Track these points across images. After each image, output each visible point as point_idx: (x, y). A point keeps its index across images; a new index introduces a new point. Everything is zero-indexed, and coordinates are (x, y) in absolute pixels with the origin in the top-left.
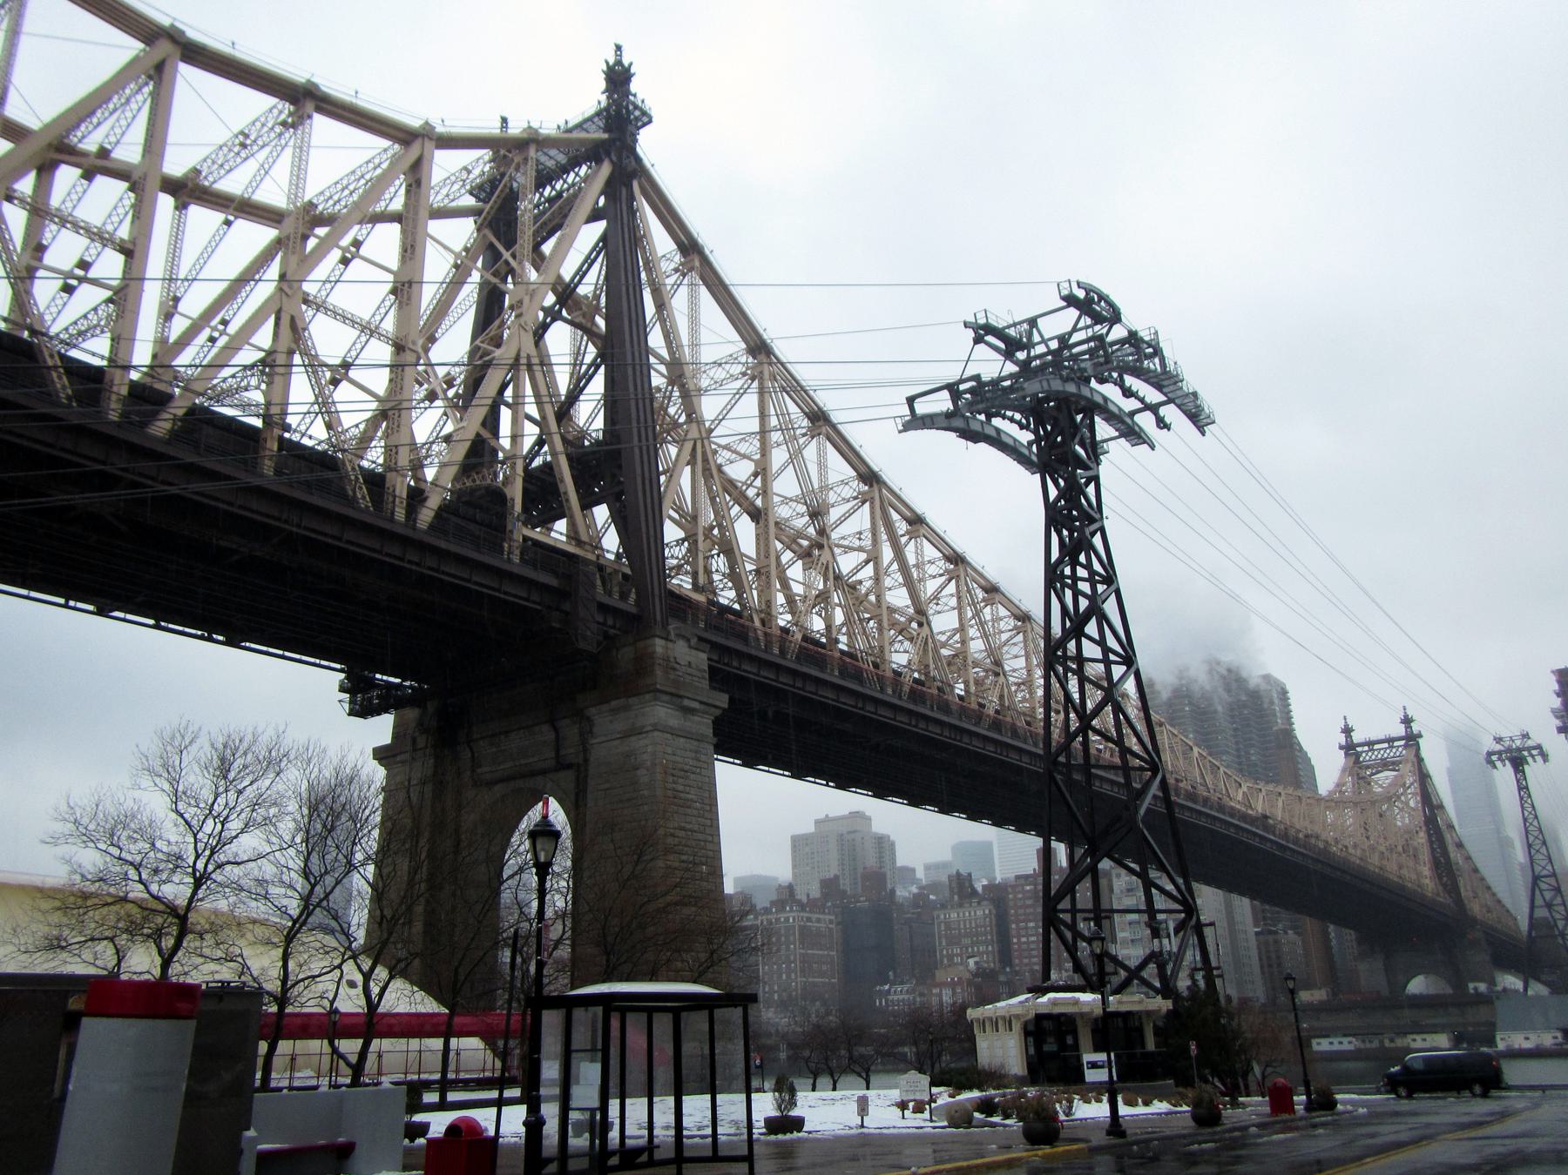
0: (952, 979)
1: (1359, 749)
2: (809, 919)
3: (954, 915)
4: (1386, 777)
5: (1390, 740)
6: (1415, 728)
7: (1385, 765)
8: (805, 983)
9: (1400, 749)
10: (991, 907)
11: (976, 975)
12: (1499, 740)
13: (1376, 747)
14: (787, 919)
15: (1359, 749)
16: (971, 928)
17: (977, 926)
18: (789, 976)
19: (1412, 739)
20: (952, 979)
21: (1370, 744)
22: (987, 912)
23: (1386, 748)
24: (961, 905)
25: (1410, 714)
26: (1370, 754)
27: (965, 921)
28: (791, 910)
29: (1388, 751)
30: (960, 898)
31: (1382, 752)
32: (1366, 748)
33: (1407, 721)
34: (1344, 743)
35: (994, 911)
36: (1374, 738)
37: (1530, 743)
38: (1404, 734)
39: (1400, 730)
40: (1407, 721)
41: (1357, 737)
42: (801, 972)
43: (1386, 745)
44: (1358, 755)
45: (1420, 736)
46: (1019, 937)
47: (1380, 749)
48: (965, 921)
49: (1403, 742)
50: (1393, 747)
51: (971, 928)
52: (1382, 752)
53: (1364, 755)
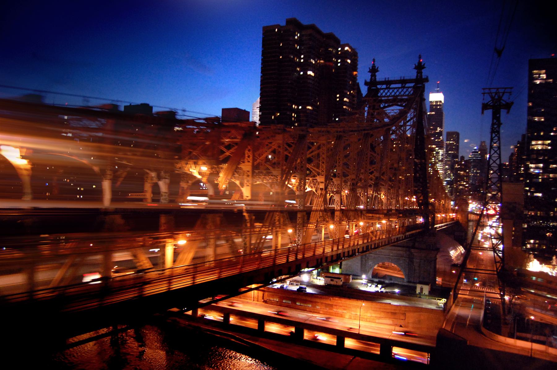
1: (379, 86)
4: (393, 110)
5: (403, 82)
7: (394, 101)
9: (410, 90)
13: (392, 86)
15: (379, 86)
21: (388, 83)
23: (399, 88)
26: (386, 91)
29: (400, 90)
31: (395, 91)
32: (384, 86)
34: (368, 80)
36: (391, 79)
38: (414, 77)
39: (413, 74)
41: (379, 77)
43: (400, 85)
44: (378, 90)
45: (427, 80)
47: (395, 88)
49: (412, 85)
50: (403, 87)
52: (395, 91)
53: (382, 91)
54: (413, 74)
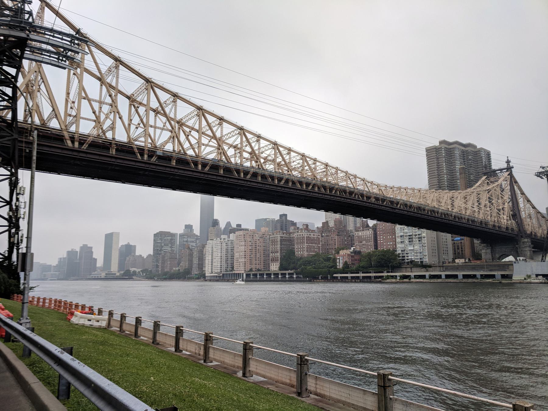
0: (343, 254)
2: (310, 235)
3: (360, 234)
6: (511, 164)
8: (308, 254)
10: (372, 231)
11: (351, 253)
12: (543, 168)
14: (302, 235)
16: (365, 238)
17: (367, 237)
18: (303, 252)
19: (509, 169)
20: (343, 254)
22: (371, 233)
24: (363, 230)
25: (509, 159)
27: (364, 236)
28: (305, 232)
30: (363, 228)
33: (508, 162)
35: (373, 232)
40: (508, 162)
42: (307, 251)
46: (380, 241)
48: (365, 235)
49: (505, 170)
51: (365, 238)
54: (505, 166)
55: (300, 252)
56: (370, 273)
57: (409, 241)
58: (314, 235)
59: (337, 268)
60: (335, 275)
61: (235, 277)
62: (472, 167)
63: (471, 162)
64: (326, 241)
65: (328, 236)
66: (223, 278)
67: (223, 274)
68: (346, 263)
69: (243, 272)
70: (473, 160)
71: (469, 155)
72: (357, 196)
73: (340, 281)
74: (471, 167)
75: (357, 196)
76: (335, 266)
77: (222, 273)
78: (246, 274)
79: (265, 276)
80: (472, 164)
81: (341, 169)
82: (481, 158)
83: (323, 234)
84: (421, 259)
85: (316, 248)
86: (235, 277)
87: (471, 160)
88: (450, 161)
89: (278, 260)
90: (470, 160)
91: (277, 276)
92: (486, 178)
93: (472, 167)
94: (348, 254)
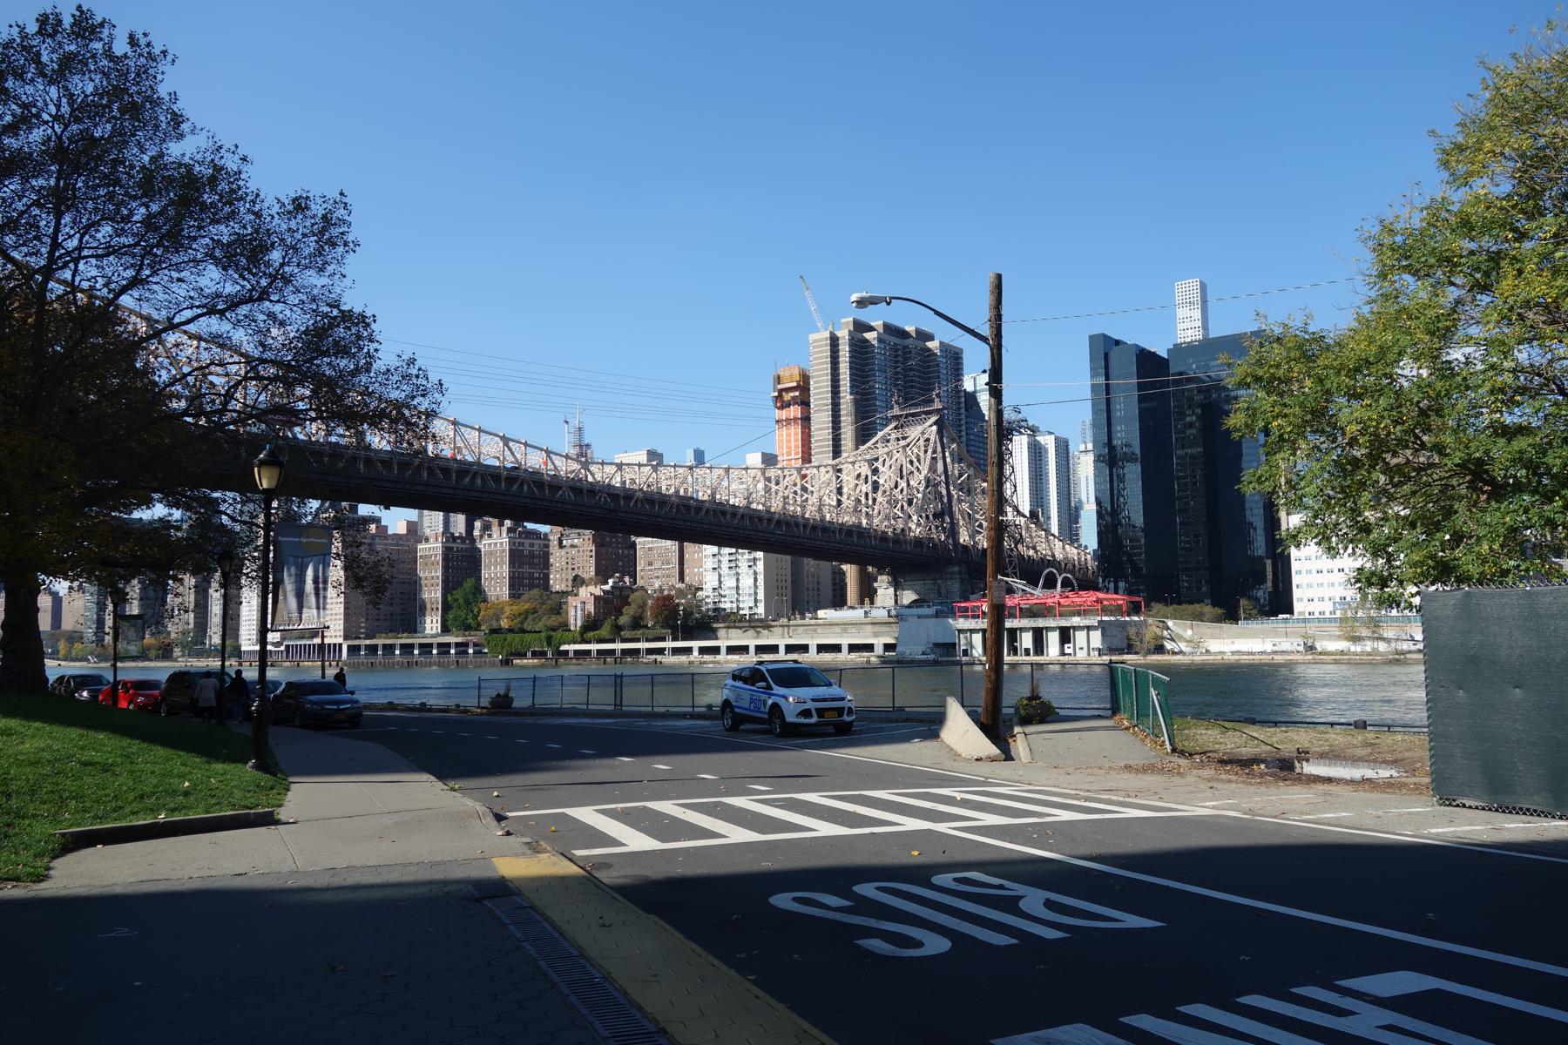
37: (1020, 416)
55: (495, 590)
56: (638, 640)
57: (730, 568)
58: (532, 545)
59: (570, 630)
60: (564, 647)
61: (335, 651)
62: (915, 387)
63: (914, 375)
64: (570, 561)
65: (576, 547)
66: (287, 657)
67: (287, 647)
68: (587, 617)
69: (340, 640)
70: (919, 371)
71: (910, 359)
72: (526, 488)
73: (574, 661)
74: (912, 387)
75: (526, 488)
76: (565, 626)
77: (285, 643)
78: (349, 646)
79: (397, 652)
80: (915, 381)
81: (487, 429)
82: (938, 365)
83: (564, 542)
84: (751, 608)
85: (536, 579)
86: (335, 651)
87: (911, 370)
88: (863, 371)
89: (437, 609)
90: (911, 370)
91: (462, 649)
92: (896, 428)
93: (915, 387)
94: (597, 598)
